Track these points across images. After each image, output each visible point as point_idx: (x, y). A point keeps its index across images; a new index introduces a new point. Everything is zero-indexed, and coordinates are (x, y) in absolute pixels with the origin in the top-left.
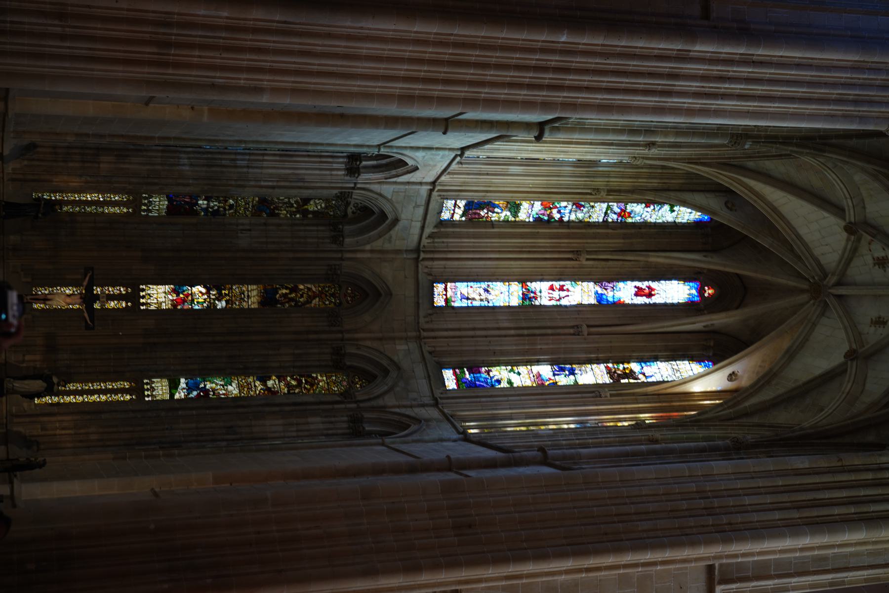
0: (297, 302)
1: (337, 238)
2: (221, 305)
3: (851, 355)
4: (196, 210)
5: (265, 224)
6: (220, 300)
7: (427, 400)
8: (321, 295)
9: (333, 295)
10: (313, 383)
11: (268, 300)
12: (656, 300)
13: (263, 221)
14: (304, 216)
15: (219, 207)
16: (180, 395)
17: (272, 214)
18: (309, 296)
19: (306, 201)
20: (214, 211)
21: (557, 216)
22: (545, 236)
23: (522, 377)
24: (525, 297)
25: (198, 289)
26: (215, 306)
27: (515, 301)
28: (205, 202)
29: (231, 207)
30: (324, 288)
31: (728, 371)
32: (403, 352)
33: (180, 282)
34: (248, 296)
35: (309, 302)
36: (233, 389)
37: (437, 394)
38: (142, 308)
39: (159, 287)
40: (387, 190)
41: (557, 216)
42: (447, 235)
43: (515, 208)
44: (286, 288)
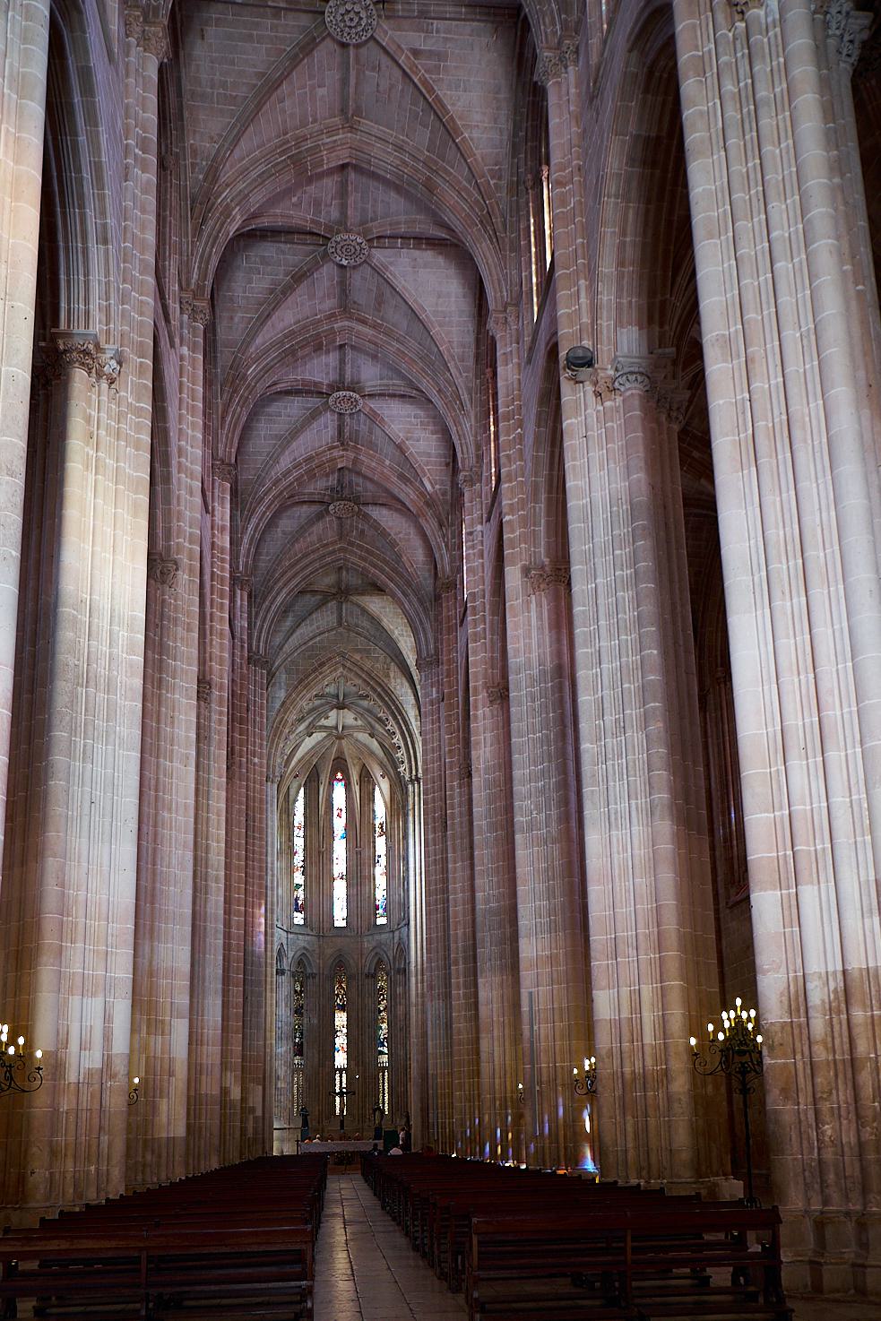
1: (313, 976)
2: (345, 1030)
3: (372, 735)
7: (391, 935)
8: (340, 983)
10: (381, 988)
11: (342, 1008)
12: (343, 806)
16: (386, 1050)
17: (302, 1007)
19: (296, 991)
21: (302, 863)
22: (311, 870)
23: (381, 881)
24: (342, 878)
27: (344, 883)
31: (380, 779)
32: (368, 944)
33: (332, 1049)
36: (384, 1026)
37: (388, 930)
40: (291, 954)
41: (302, 863)
42: (311, 921)
43: (298, 886)
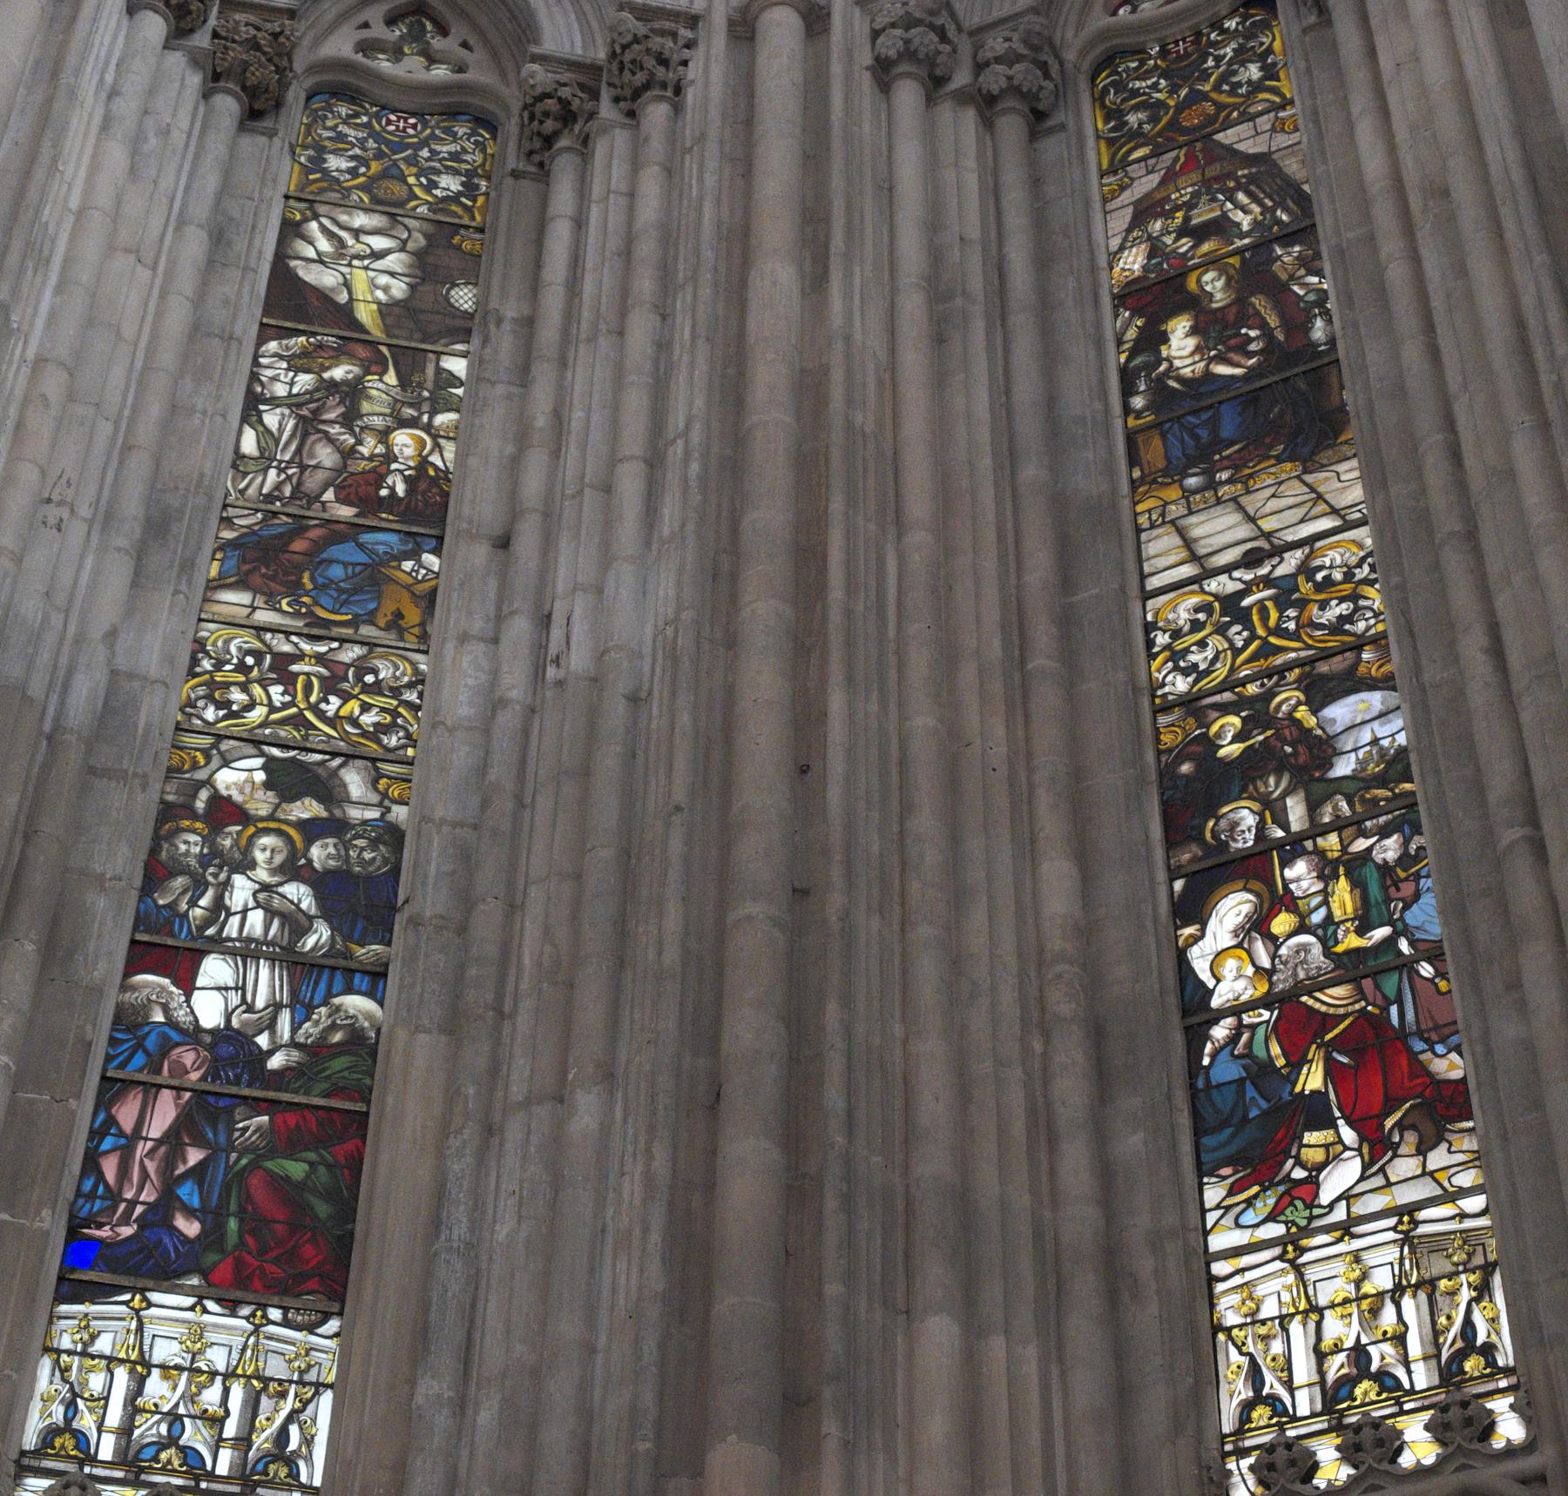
0: (1267, 238)
4: (316, 1052)
5: (504, 543)
6: (1323, 748)
9: (1182, 69)
13: (480, 554)
14: (465, 335)
15: (293, 869)
18: (1209, 187)
20: (327, 912)
25: (1223, 953)
26: (1396, 765)
28: (215, 969)
29: (287, 780)
30: (1120, 138)
34: (1252, 559)
35: (1263, 174)
38: (1510, 1429)
39: (1230, 1311)
44: (1154, 338)
